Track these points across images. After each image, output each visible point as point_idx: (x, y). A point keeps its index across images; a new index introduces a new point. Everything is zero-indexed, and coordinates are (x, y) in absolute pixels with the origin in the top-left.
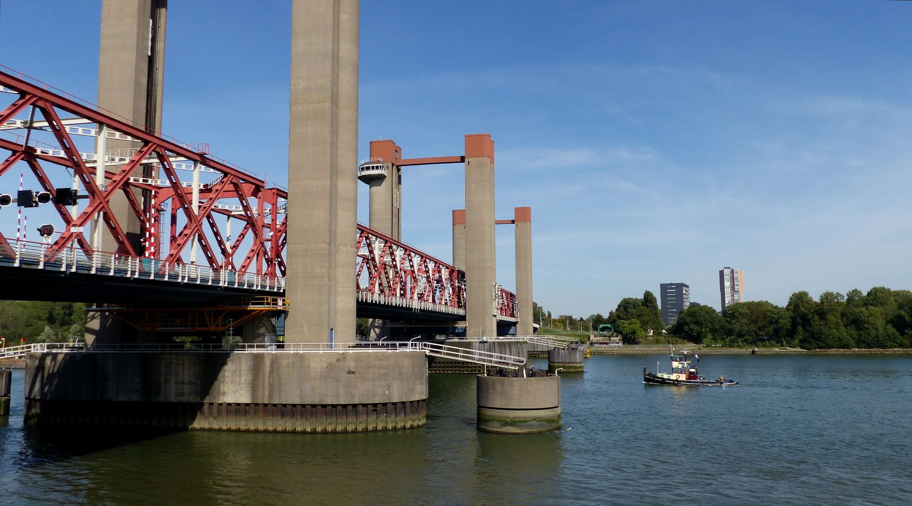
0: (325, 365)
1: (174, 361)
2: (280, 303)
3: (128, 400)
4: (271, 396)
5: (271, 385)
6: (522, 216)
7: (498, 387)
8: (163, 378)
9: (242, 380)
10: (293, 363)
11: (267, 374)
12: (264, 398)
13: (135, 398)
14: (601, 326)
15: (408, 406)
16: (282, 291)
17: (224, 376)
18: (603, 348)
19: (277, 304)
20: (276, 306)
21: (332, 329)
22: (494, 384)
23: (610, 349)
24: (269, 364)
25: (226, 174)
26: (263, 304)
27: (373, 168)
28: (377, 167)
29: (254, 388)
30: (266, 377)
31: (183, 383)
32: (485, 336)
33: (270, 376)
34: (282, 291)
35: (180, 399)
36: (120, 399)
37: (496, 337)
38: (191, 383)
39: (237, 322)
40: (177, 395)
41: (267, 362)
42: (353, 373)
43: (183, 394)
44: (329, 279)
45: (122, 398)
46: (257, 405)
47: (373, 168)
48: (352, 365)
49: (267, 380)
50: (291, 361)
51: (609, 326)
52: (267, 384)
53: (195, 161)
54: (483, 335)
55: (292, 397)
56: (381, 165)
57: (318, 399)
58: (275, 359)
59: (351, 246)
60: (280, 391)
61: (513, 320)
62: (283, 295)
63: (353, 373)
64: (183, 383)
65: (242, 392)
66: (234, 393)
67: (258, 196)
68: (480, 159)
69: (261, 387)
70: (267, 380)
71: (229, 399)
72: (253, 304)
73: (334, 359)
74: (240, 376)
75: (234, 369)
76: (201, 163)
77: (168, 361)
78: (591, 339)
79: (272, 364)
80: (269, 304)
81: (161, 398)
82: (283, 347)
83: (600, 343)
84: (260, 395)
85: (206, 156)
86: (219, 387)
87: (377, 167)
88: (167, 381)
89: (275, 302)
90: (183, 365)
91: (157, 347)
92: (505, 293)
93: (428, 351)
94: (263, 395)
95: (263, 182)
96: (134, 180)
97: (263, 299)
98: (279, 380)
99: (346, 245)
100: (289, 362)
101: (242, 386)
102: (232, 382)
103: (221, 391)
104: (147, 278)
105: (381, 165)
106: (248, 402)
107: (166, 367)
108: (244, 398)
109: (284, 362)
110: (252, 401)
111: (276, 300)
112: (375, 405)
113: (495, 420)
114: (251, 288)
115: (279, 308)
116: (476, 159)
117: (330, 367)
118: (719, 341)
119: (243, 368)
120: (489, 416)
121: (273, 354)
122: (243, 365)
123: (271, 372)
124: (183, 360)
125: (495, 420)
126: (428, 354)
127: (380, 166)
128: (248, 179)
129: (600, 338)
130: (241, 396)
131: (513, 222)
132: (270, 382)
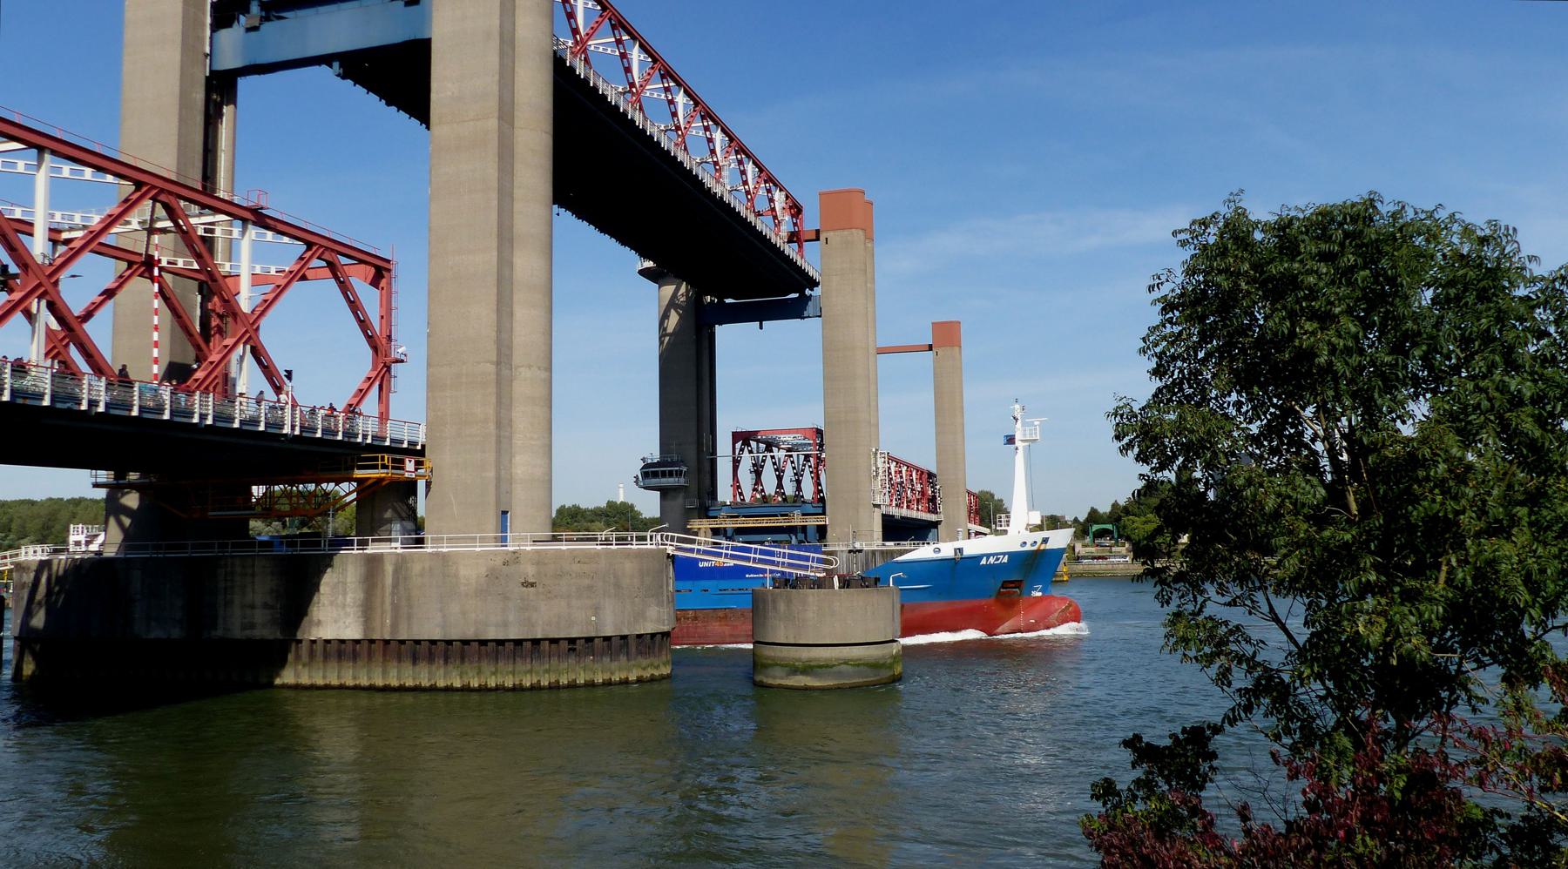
0: (483, 571)
1: (238, 569)
2: (410, 465)
4: (395, 625)
5: (396, 608)
6: (946, 336)
7: (782, 606)
9: (348, 600)
10: (431, 569)
11: (388, 590)
13: (176, 633)
14: (1095, 527)
15: (632, 643)
16: (419, 447)
18: (1098, 565)
19: (403, 469)
20: (401, 472)
21: (505, 513)
23: (1110, 567)
24: (391, 573)
25: (309, 245)
26: (375, 467)
29: (368, 610)
30: (387, 594)
31: (253, 607)
32: (858, 540)
33: (393, 594)
34: (419, 447)
35: (248, 633)
36: (152, 635)
37: (881, 542)
38: (266, 606)
40: (244, 628)
41: (389, 569)
42: (532, 585)
44: (499, 425)
45: (156, 633)
46: (372, 641)
48: (530, 571)
50: (427, 565)
51: (1109, 527)
52: (388, 606)
53: (245, 221)
54: (855, 536)
55: (428, 627)
57: (472, 630)
58: (401, 563)
59: (539, 368)
60: (409, 617)
61: (933, 518)
62: (422, 453)
63: (532, 585)
64: (253, 607)
65: (348, 621)
66: (336, 621)
67: (381, 285)
68: (846, 232)
69: (379, 611)
70: (388, 600)
72: (361, 468)
74: (345, 594)
75: (336, 580)
76: (254, 224)
78: (1077, 550)
79: (397, 571)
80: (387, 467)
81: (219, 632)
83: (1094, 558)
84: (377, 624)
85: (264, 211)
89: (399, 465)
90: (253, 575)
92: (917, 471)
93: (671, 548)
94: (383, 624)
95: (388, 261)
96: (169, 263)
97: (376, 459)
98: (409, 598)
99: (530, 367)
100: (424, 568)
101: (348, 610)
102: (332, 603)
103: (315, 619)
104: (125, 413)
107: (226, 580)
108: (351, 630)
109: (416, 568)
110: (365, 635)
111: (402, 461)
112: (572, 641)
113: (777, 665)
114: (352, 440)
115: (407, 475)
116: (838, 233)
117: (493, 575)
119: (349, 580)
120: (768, 658)
121: (398, 554)
122: (349, 574)
123: (395, 585)
124: (253, 566)
125: (777, 665)
126: (671, 553)
128: (361, 257)
129: (1093, 549)
130: (347, 627)
131: (930, 348)
132: (393, 603)
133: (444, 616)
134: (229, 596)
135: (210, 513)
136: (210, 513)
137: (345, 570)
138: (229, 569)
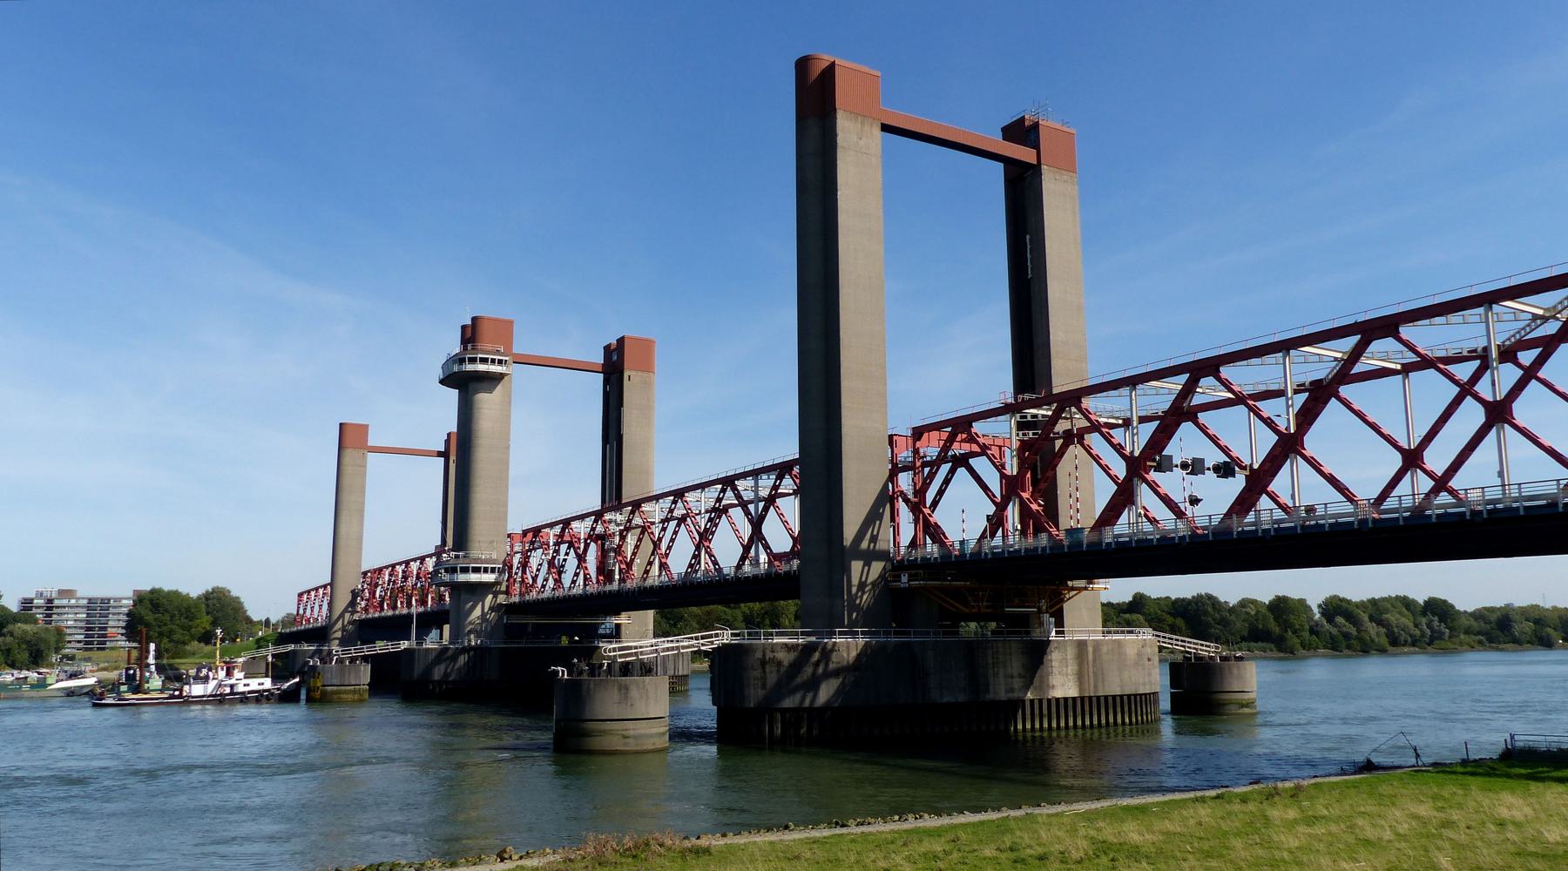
1: (1001, 650)
3: (954, 701)
4: (1096, 686)
5: (1095, 674)
8: (991, 672)
9: (1069, 671)
10: (1112, 650)
11: (1091, 664)
13: (961, 698)
17: (1052, 667)
22: (1229, 669)
27: (493, 361)
28: (500, 362)
29: (1080, 677)
31: (1012, 677)
33: (1093, 666)
35: (1010, 695)
36: (945, 700)
38: (1020, 676)
39: (1058, 607)
40: (1007, 692)
41: (1090, 649)
47: (493, 361)
49: (1091, 669)
50: (1110, 647)
52: (1091, 675)
56: (507, 358)
60: (1103, 681)
64: (1012, 677)
65: (1071, 684)
66: (1063, 685)
68: (645, 374)
69: (1086, 677)
71: (1058, 693)
73: (1140, 646)
74: (1067, 666)
77: (995, 650)
79: (1094, 651)
81: (991, 696)
82: (1063, 632)
86: (1048, 679)
87: (500, 362)
88: (996, 675)
90: (1011, 654)
91: (928, 633)
103: (1051, 684)
105: (507, 358)
106: (1076, 695)
107: (993, 658)
109: (1104, 649)
110: (1080, 693)
116: (639, 373)
119: (1069, 657)
120: (1224, 700)
123: (1094, 661)
124: (1010, 648)
127: (506, 361)
133: (1121, 680)
135: (1007, 609)
136: (1007, 609)
137: (1066, 650)
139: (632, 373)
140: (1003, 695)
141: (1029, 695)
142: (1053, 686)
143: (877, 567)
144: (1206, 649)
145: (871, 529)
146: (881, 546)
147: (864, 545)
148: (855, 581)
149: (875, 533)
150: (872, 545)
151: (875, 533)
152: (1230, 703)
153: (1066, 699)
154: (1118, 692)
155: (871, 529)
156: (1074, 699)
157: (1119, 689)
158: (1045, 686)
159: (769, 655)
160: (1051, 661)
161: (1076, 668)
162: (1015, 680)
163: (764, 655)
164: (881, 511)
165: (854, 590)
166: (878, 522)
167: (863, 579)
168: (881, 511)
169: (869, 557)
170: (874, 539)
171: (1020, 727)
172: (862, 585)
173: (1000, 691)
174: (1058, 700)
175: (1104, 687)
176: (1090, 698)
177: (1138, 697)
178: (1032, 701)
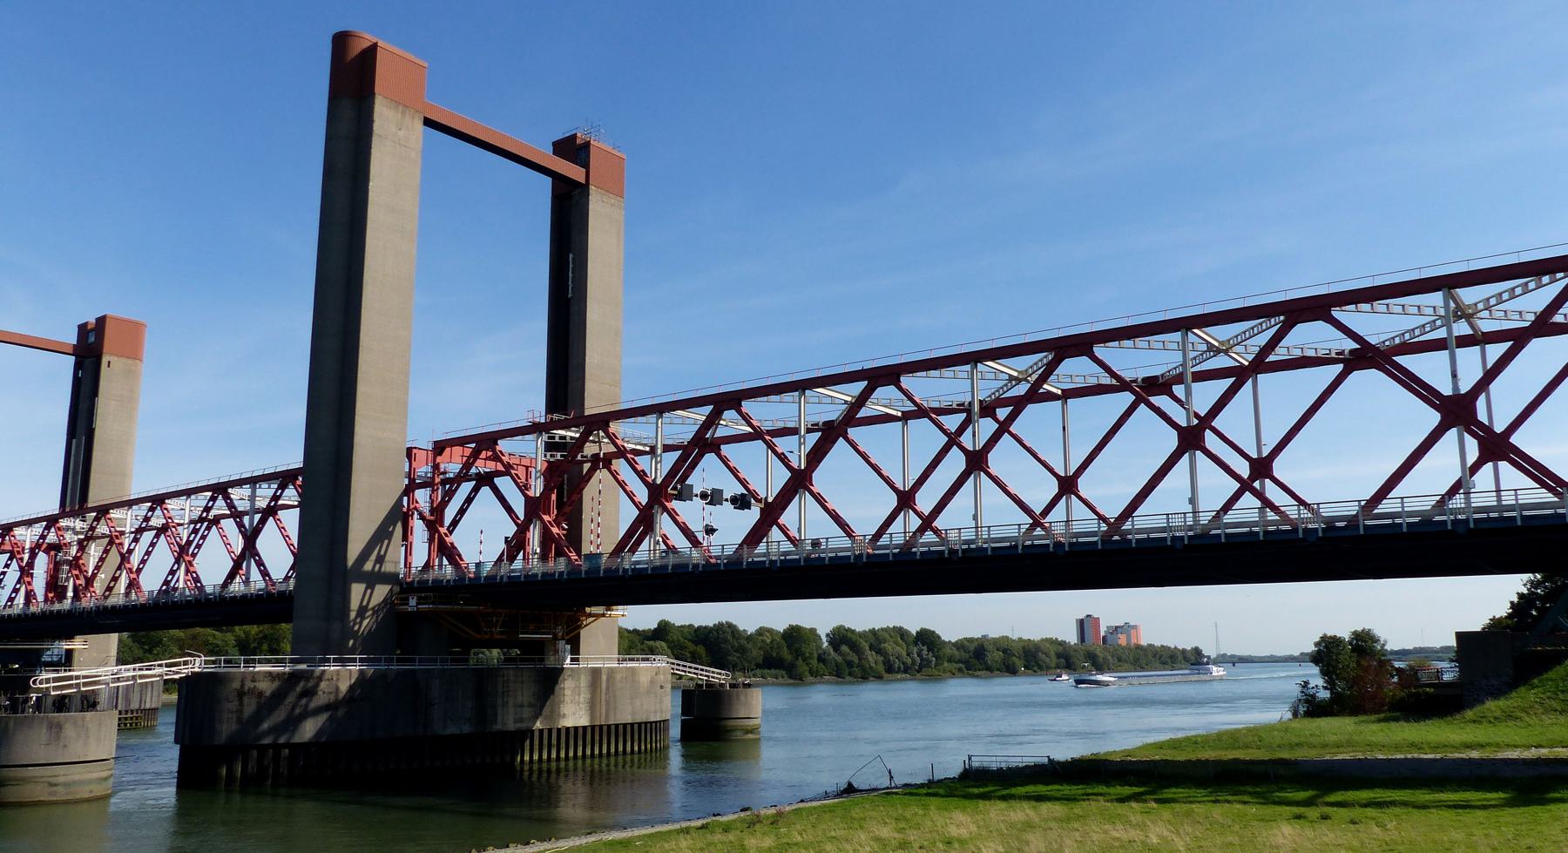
1: (512, 678)
3: (458, 732)
5: (608, 703)
7: (742, 698)
8: (500, 701)
10: (626, 677)
12: (601, 720)
13: (467, 729)
17: (564, 695)
22: (737, 695)
29: (592, 706)
38: (530, 705)
41: (604, 677)
43: (521, 720)
45: (452, 730)
52: (604, 703)
60: (615, 710)
64: (522, 706)
66: (574, 714)
69: (599, 706)
74: (579, 695)
81: (499, 727)
82: (577, 660)
86: (559, 708)
88: (505, 704)
90: (522, 683)
91: (436, 660)
98: (615, 697)
103: (562, 713)
106: (587, 724)
109: (618, 677)
110: (591, 722)
116: (122, 359)
118: (551, 662)
119: (582, 685)
120: (733, 726)
123: (607, 689)
124: (522, 676)
133: (633, 708)
134: (505, 699)
137: (580, 678)
138: (505, 678)
139: (113, 359)
140: (511, 726)
141: (538, 725)
142: (564, 714)
143: (381, 592)
144: (718, 676)
145: (378, 548)
146: (388, 567)
147: (368, 566)
148: (355, 604)
149: (382, 553)
150: (378, 566)
151: (382, 553)
152: (735, 729)
153: (576, 728)
154: (629, 720)
155: (378, 548)
156: (585, 728)
157: (630, 717)
158: (555, 714)
159: (249, 685)
160: (564, 689)
161: (589, 696)
162: (525, 709)
163: (243, 685)
164: (391, 529)
165: (353, 615)
166: (386, 541)
167: (365, 603)
168: (391, 529)
169: (372, 580)
170: (380, 560)
171: (527, 758)
172: (362, 611)
173: (508, 721)
174: (568, 729)
175: (615, 717)
176: (601, 726)
177: (649, 725)
178: (541, 731)
